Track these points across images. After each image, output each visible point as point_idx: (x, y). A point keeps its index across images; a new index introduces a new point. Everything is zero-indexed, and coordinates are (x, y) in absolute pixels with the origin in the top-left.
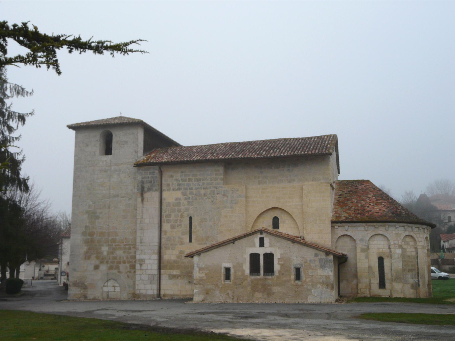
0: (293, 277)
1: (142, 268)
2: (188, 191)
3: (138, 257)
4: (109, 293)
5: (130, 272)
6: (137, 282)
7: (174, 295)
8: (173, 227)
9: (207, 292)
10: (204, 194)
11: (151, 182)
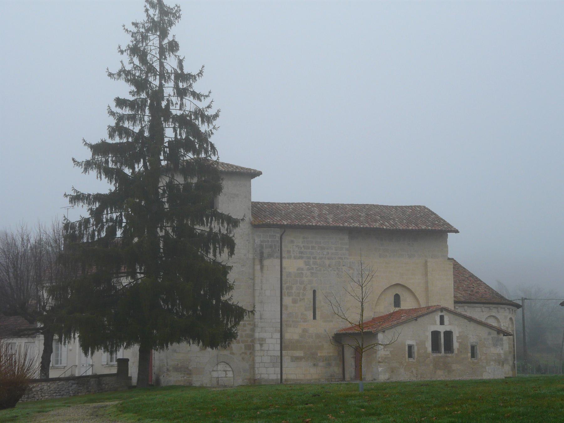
0: (470, 355)
1: (263, 348)
2: (312, 261)
3: (257, 335)
4: (220, 379)
5: (246, 353)
6: (257, 365)
7: (297, 380)
8: (294, 302)
9: (392, 370)
10: (329, 266)
11: (271, 247)
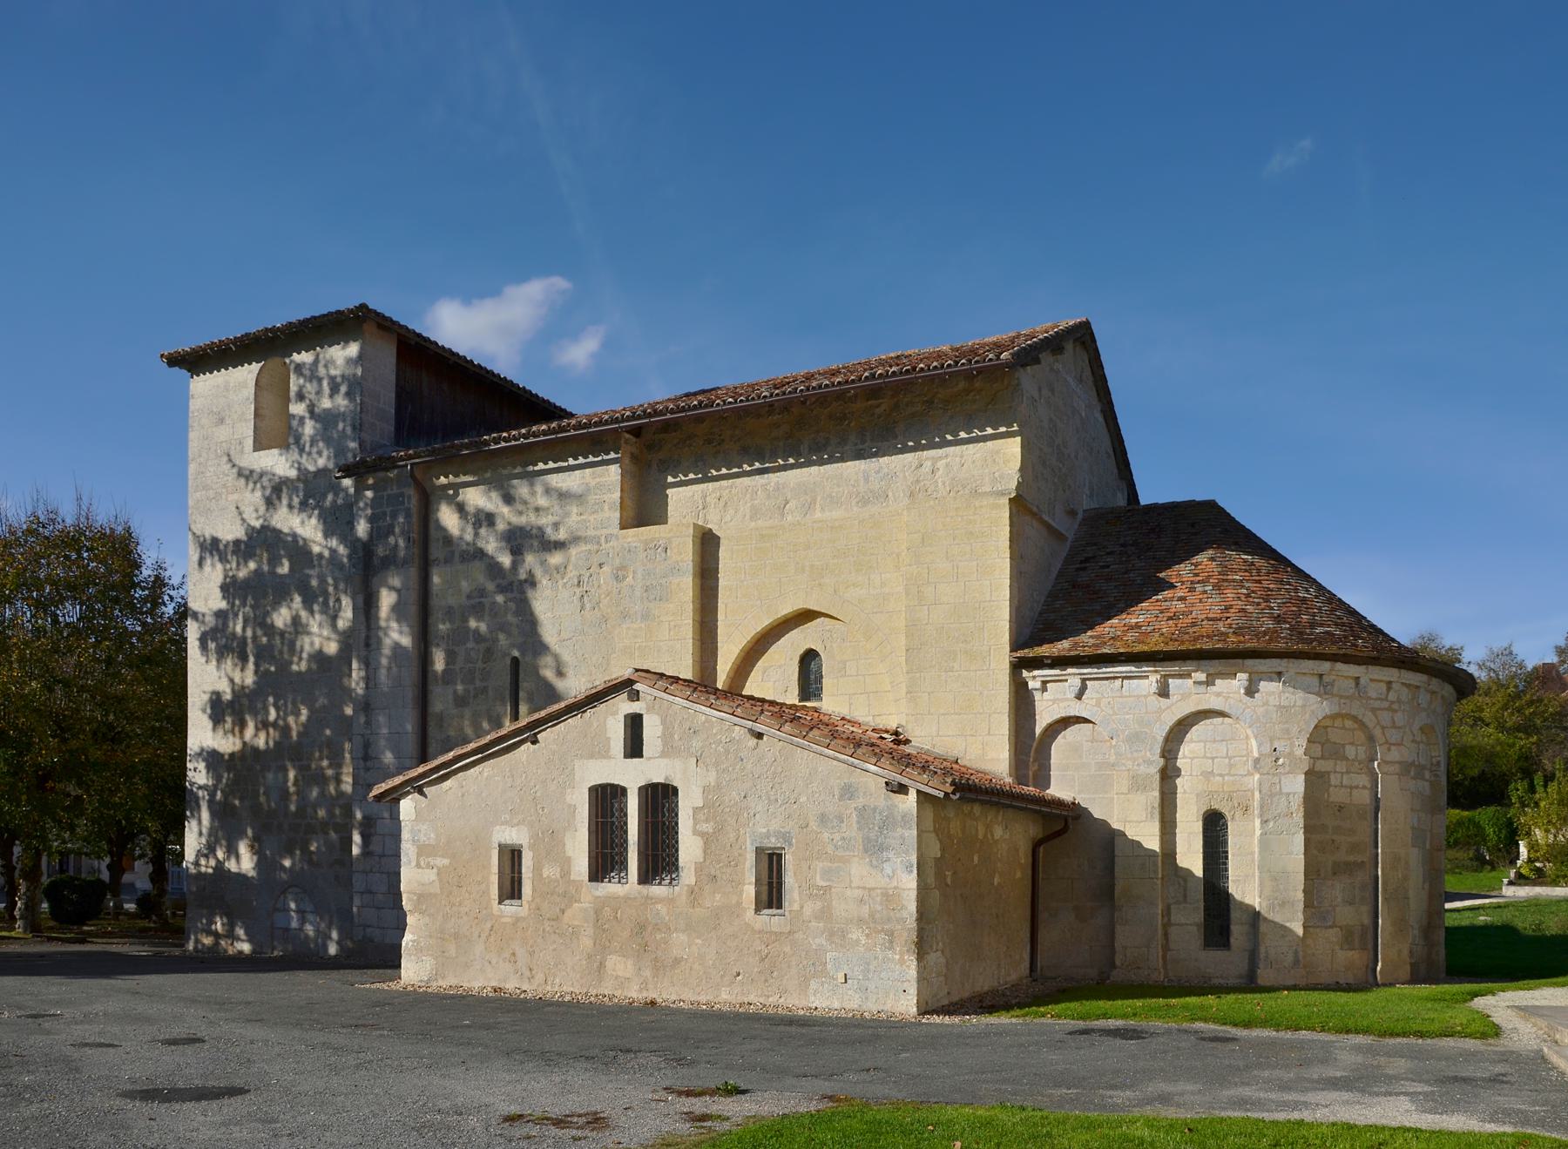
0: (750, 891)
